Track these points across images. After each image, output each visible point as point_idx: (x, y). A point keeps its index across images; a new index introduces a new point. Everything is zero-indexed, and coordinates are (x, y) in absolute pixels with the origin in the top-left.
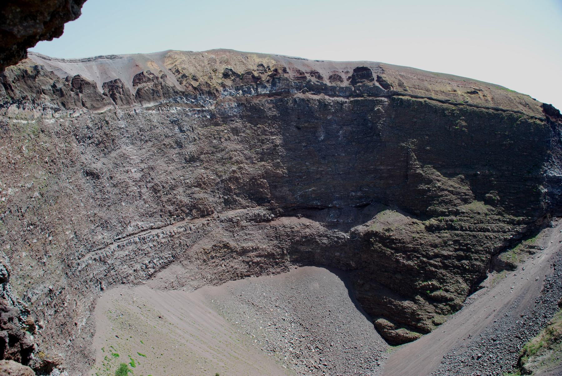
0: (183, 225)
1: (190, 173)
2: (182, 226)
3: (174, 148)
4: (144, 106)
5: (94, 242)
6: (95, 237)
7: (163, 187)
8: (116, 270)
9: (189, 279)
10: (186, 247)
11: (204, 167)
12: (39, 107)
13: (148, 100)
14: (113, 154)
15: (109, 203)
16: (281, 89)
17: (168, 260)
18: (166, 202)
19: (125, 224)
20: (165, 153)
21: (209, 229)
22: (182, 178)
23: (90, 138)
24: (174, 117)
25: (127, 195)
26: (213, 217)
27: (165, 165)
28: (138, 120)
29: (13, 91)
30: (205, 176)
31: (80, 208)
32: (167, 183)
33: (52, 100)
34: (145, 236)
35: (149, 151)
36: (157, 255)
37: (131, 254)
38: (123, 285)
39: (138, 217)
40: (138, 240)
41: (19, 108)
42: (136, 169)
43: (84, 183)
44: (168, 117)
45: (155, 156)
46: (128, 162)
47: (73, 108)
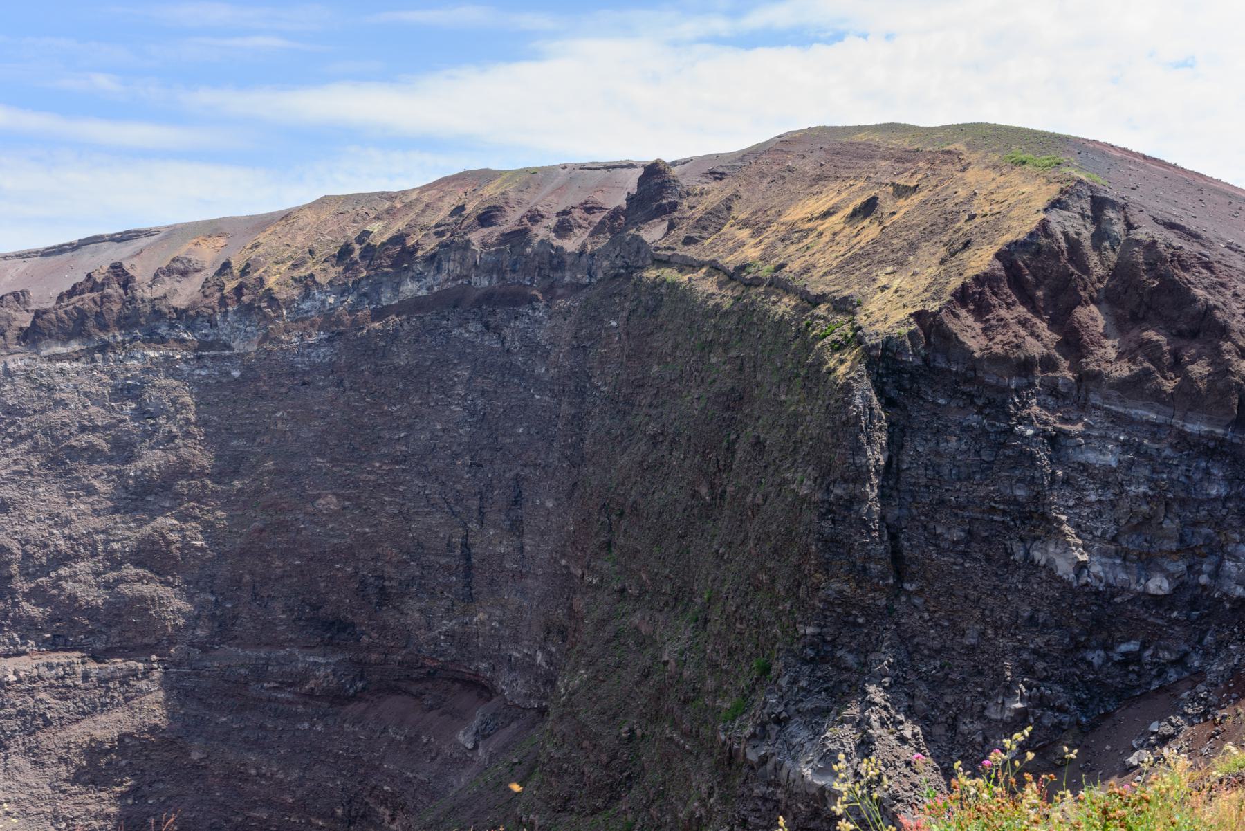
0: (63, 661)
1: (132, 525)
2: (55, 661)
3: (110, 460)
4: (45, 352)
7: (27, 556)
10: (40, 722)
11: (181, 512)
13: (61, 336)
16: (454, 280)
18: (24, 594)
20: (68, 472)
21: (143, 685)
22: (97, 537)
24: (127, 378)
26: (170, 656)
27: (61, 500)
28: (8, 387)
30: (174, 536)
32: (46, 546)
35: (15, 462)
44: (113, 377)
45: (32, 475)
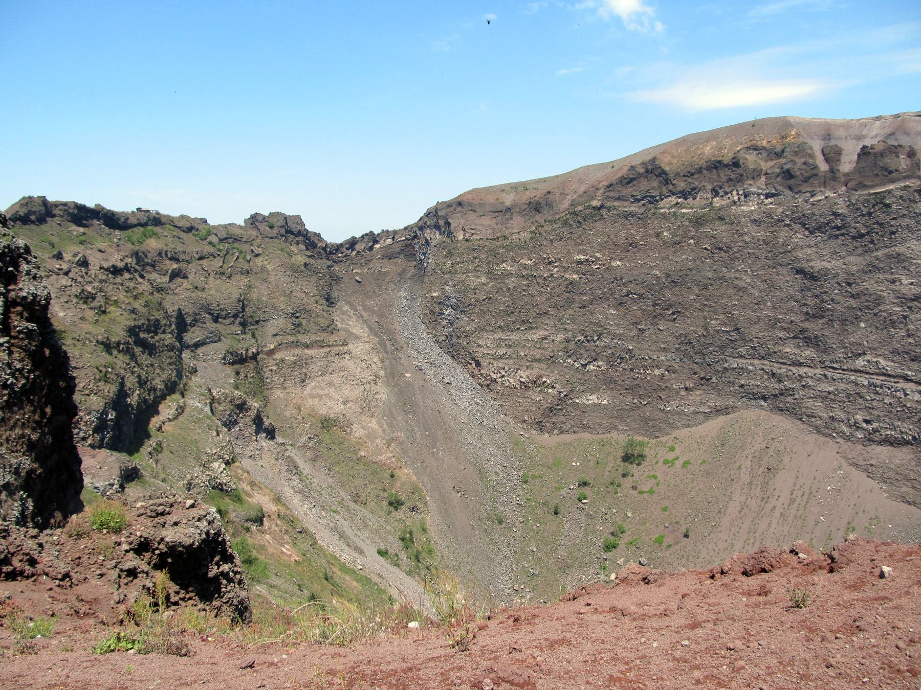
5: (775, 353)
6: (780, 348)
8: (796, 399)
9: (908, 480)
12: (729, 195)
14: (879, 253)
15: (832, 315)
17: (903, 437)
19: (852, 352)
23: (838, 228)
25: (875, 315)
29: (673, 185)
31: (761, 306)
33: (766, 185)
34: (878, 383)
36: (887, 420)
37: (840, 395)
38: (799, 422)
39: (887, 353)
40: (866, 383)
41: (686, 199)
42: (916, 280)
43: (787, 281)
46: (904, 267)
47: (808, 189)
